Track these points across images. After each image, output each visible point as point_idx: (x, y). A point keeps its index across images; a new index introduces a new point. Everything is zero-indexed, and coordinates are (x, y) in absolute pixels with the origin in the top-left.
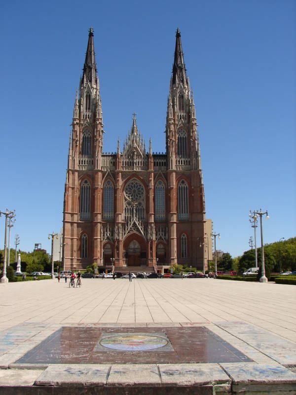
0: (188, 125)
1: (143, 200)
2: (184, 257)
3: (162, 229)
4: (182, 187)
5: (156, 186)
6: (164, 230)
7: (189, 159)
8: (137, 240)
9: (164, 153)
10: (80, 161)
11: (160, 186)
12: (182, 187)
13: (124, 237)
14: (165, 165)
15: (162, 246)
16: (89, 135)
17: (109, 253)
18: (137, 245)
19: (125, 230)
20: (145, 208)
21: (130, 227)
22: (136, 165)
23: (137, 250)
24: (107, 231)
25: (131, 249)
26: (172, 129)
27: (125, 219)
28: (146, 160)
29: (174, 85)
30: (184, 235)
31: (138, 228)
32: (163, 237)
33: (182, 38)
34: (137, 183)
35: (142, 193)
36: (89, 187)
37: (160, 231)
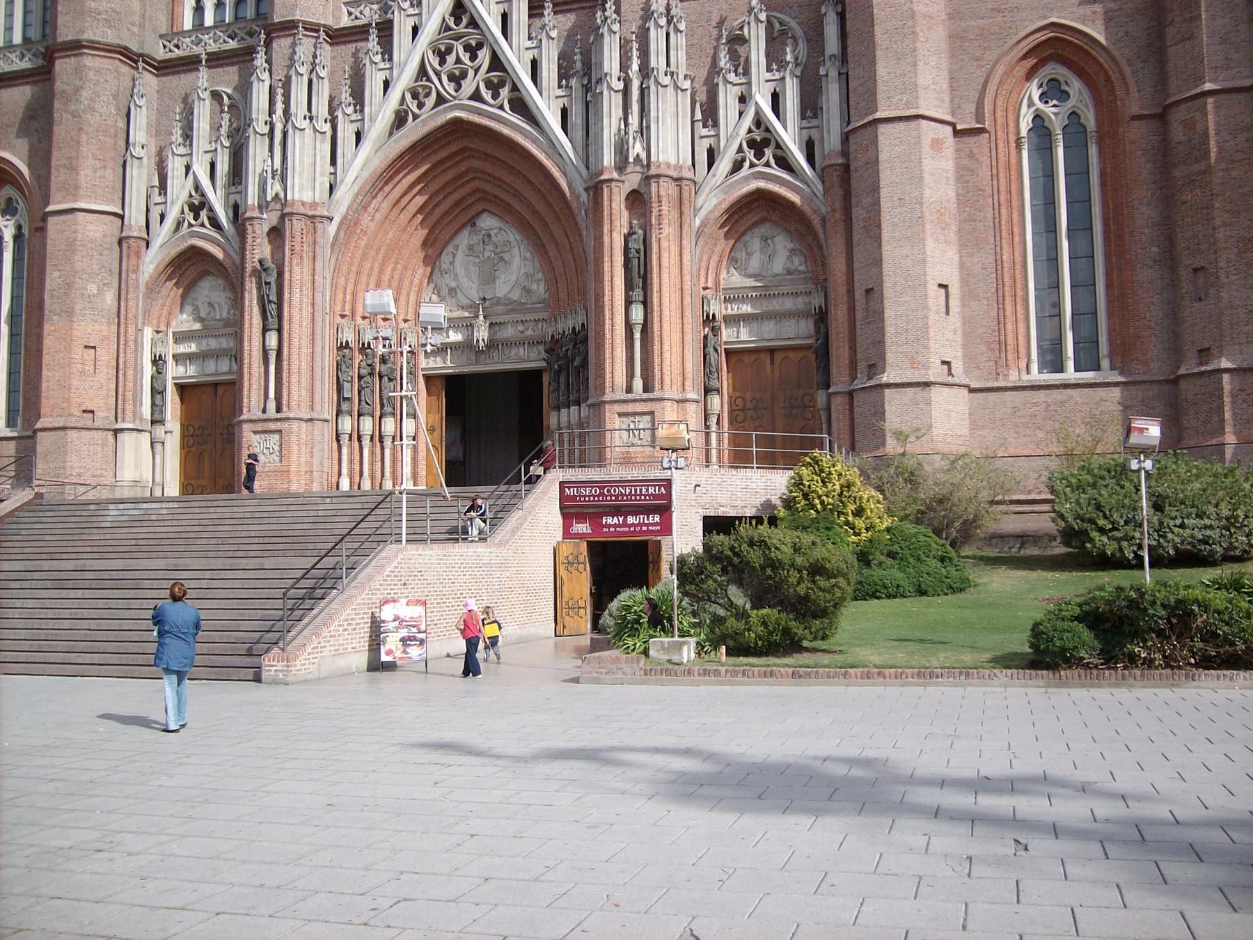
2: (1071, 373)
8: (505, 211)
31: (497, 63)
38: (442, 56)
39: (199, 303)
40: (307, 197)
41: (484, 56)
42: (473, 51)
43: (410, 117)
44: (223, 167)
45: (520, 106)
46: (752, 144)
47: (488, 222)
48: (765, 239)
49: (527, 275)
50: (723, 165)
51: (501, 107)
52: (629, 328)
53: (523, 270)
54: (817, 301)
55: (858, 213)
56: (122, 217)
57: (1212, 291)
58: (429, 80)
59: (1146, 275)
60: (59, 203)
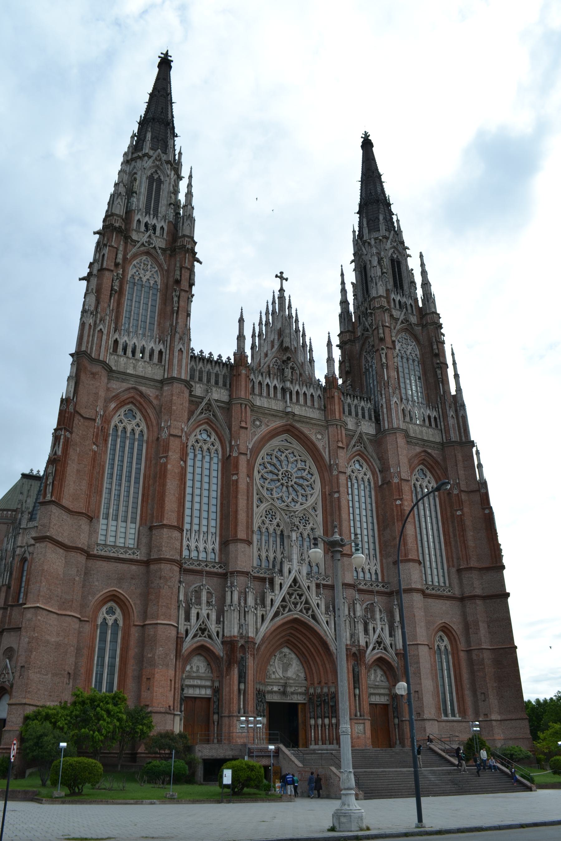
1: (314, 509)
3: (380, 611)
10: (116, 342)
13: (263, 629)
14: (370, 419)
15: (379, 672)
17: (203, 692)
19: (263, 605)
21: (278, 596)
24: (199, 603)
26: (387, 324)
31: (307, 602)
32: (387, 640)
38: (291, 595)
39: (194, 666)
40: (252, 636)
41: (303, 598)
42: (300, 596)
43: (281, 614)
44: (213, 617)
45: (314, 617)
46: (377, 642)
47: (286, 650)
48: (375, 670)
49: (298, 670)
50: (370, 648)
51: (309, 617)
52: (355, 695)
53: (296, 669)
55: (411, 670)
56: (177, 628)
57: (487, 699)
58: (286, 602)
59: (468, 693)
60: (162, 620)
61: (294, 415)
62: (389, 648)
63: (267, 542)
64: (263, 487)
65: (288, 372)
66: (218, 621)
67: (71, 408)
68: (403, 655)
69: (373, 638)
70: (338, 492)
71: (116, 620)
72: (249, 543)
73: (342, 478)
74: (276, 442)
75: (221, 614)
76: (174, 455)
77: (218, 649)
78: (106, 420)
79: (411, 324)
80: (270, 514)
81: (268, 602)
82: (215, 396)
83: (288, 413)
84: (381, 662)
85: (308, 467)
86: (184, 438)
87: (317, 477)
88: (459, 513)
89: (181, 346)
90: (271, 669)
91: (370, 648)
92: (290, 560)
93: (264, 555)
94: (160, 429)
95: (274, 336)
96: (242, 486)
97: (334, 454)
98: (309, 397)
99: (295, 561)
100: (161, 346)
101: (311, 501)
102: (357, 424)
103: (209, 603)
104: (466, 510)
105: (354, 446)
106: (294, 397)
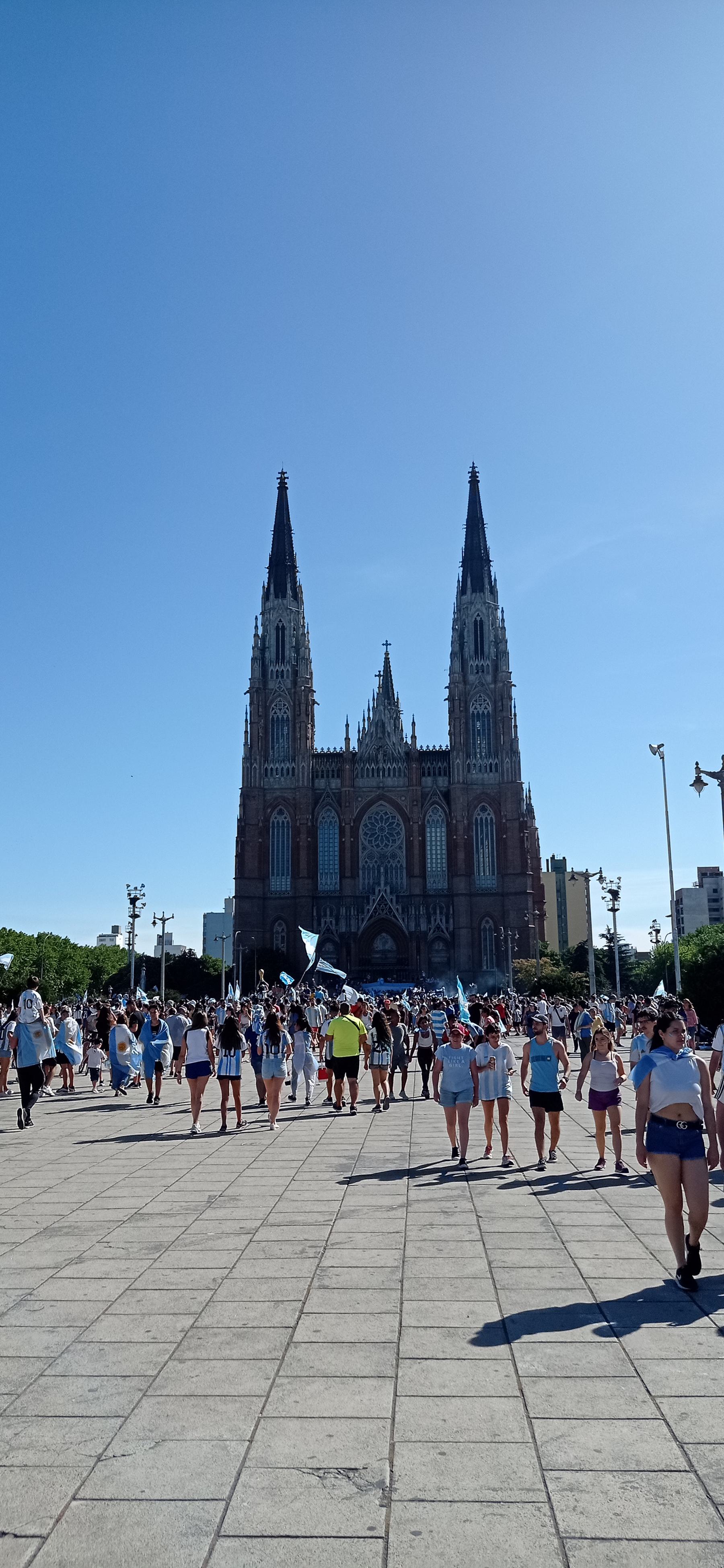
0: (492, 686)
1: (400, 848)
3: (441, 908)
4: (481, 819)
5: (427, 817)
6: (445, 910)
7: (496, 760)
8: (387, 932)
9: (444, 748)
11: (435, 817)
12: (481, 819)
15: (441, 944)
16: (285, 713)
18: (390, 945)
19: (363, 913)
20: (404, 865)
22: (384, 775)
23: (389, 955)
25: (377, 952)
27: (364, 889)
28: (405, 764)
29: (464, 597)
30: (487, 922)
32: (443, 927)
33: (481, 486)
34: (386, 813)
35: (398, 834)
36: (288, 822)
37: (435, 913)
38: (380, 905)
42: (386, 905)
44: (334, 922)
45: (395, 916)
47: (384, 934)
50: (432, 931)
54: (448, 955)
61: (383, 788)
62: (445, 931)
63: (369, 873)
64: (365, 839)
65: (380, 756)
66: (337, 924)
67: (243, 824)
68: (453, 934)
69: (433, 926)
70: (412, 836)
71: (283, 929)
72: (354, 876)
73: (416, 827)
74: (374, 808)
75: (337, 920)
76: (303, 836)
77: (337, 939)
78: (267, 820)
79: (483, 685)
80: (370, 856)
81: (366, 911)
82: (333, 786)
83: (379, 788)
84: (439, 938)
85: (396, 821)
86: (309, 824)
87: (403, 826)
88: (504, 836)
89: (303, 764)
90: (375, 946)
91: (432, 931)
92: (379, 885)
93: (366, 881)
94: (296, 820)
95: (373, 729)
96: (348, 845)
97: (412, 812)
98: (397, 770)
99: (382, 885)
100: (293, 764)
101: (398, 843)
102: (435, 782)
103: (331, 915)
104: (509, 834)
105: (431, 798)
106: (386, 773)
